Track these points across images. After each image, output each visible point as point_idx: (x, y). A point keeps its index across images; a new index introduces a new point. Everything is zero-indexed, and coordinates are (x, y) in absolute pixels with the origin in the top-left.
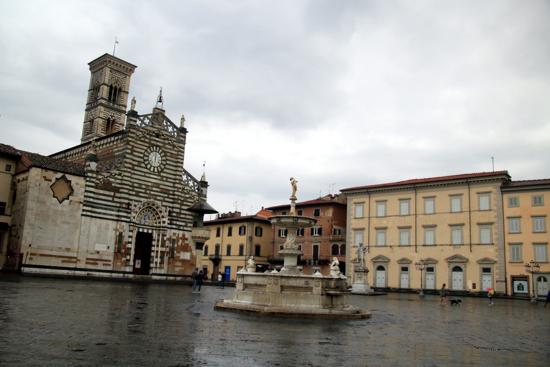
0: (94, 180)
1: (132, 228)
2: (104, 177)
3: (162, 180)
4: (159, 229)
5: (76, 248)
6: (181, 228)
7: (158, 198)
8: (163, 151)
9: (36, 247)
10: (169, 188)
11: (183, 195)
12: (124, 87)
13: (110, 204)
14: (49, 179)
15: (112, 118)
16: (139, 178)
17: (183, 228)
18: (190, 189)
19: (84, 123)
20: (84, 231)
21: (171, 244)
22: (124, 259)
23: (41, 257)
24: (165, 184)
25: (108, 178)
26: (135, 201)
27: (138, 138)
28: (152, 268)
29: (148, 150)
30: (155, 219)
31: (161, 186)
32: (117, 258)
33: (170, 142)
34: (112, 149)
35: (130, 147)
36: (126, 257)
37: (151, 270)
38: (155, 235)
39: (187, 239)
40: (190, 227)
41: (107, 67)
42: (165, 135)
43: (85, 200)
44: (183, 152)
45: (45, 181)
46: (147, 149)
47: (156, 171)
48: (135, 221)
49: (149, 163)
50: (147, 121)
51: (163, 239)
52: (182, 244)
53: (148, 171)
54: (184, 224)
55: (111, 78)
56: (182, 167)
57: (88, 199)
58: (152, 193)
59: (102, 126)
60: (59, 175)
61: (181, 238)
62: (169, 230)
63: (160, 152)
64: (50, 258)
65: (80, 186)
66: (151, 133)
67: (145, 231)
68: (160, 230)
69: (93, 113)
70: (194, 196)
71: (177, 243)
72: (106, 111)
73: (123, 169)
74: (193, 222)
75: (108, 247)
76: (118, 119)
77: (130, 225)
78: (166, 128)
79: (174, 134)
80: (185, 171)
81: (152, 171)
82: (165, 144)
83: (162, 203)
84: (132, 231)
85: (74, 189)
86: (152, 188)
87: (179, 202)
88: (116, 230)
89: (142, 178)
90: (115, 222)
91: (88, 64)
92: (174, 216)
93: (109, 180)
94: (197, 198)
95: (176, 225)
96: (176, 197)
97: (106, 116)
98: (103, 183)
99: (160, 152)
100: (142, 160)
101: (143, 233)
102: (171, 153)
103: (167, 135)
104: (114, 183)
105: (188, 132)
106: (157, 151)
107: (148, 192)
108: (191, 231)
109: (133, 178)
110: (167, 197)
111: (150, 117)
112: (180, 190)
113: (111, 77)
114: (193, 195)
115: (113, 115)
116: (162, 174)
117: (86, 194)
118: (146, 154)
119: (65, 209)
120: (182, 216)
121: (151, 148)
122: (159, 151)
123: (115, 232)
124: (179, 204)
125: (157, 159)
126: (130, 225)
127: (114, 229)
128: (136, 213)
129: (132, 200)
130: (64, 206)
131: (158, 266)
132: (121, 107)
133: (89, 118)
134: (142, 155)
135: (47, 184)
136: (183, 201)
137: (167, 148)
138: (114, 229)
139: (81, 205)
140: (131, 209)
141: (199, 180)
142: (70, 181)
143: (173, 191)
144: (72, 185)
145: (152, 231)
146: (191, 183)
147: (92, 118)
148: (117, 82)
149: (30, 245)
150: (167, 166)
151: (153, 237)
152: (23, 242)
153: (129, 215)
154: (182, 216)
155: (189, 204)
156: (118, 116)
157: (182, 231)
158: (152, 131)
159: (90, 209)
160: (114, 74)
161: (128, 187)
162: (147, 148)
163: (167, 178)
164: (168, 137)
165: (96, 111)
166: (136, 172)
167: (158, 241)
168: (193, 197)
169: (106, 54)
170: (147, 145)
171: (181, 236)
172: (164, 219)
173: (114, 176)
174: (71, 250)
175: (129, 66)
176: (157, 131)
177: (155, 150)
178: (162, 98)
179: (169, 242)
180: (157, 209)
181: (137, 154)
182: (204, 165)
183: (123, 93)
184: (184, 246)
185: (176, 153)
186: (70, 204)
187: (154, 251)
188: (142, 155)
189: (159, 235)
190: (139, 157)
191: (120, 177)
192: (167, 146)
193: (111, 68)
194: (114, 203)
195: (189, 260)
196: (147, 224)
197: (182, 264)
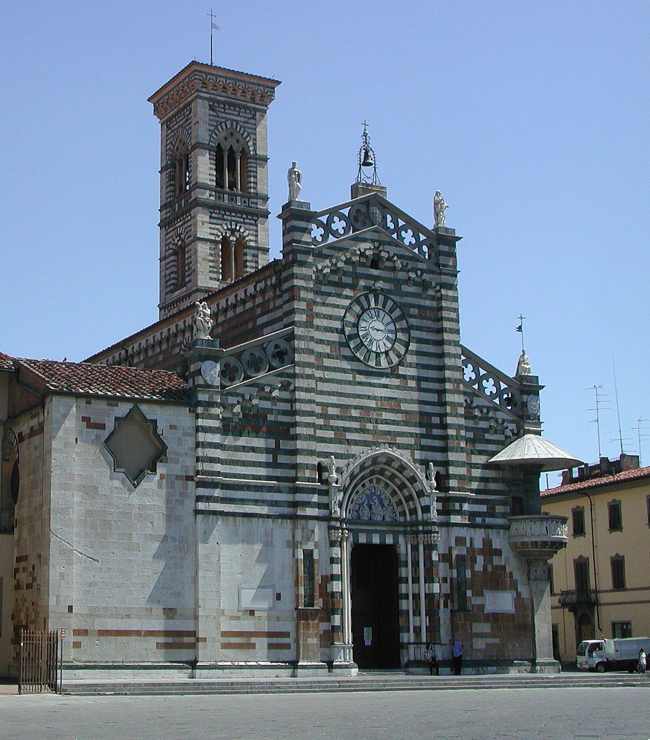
2: (243, 398)
4: (414, 529)
5: (192, 606)
6: (479, 520)
7: (400, 440)
8: (396, 305)
9: (86, 611)
10: (429, 409)
12: (255, 145)
14: (98, 421)
15: (233, 234)
17: (483, 521)
18: (491, 405)
19: (161, 260)
21: (455, 571)
22: (324, 626)
23: (102, 638)
26: (338, 456)
27: (321, 278)
28: (405, 646)
30: (399, 503)
31: (404, 406)
32: (307, 626)
33: (412, 275)
34: (254, 319)
35: (303, 305)
37: (403, 652)
38: (402, 550)
39: (498, 553)
40: (504, 515)
41: (200, 97)
43: (200, 468)
44: (455, 299)
50: (339, 225)
51: (428, 557)
52: (485, 567)
53: (362, 367)
54: (483, 508)
55: (216, 127)
56: (457, 344)
57: (207, 466)
58: (381, 427)
59: (210, 261)
60: (123, 409)
61: (482, 552)
64: (124, 639)
65: (181, 432)
66: (355, 259)
67: (376, 540)
68: (417, 533)
69: (179, 231)
72: (214, 218)
73: (291, 371)
74: (510, 500)
75: (278, 597)
76: (249, 235)
78: (395, 236)
79: (420, 250)
80: (465, 352)
82: (398, 283)
83: (413, 455)
85: (165, 442)
87: (463, 444)
88: (293, 545)
89: (348, 389)
90: (288, 523)
91: (149, 100)
92: (453, 489)
94: (512, 426)
96: (451, 432)
97: (215, 232)
98: (241, 416)
101: (369, 546)
102: (419, 307)
103: (400, 257)
105: (459, 239)
107: (370, 426)
108: (507, 528)
111: (346, 212)
113: (215, 123)
114: (500, 421)
115: (233, 227)
117: (200, 452)
119: (148, 502)
122: (384, 306)
123: (291, 550)
124: (462, 450)
126: (330, 528)
127: (288, 542)
129: (327, 455)
131: (424, 640)
132: (255, 201)
133: (171, 246)
134: (337, 325)
135: (94, 438)
137: (407, 294)
138: (288, 542)
139: (191, 484)
140: (326, 482)
141: (512, 374)
142: (154, 422)
144: (159, 432)
145: (396, 539)
146: (489, 387)
147: (180, 243)
148: (232, 134)
149: (70, 609)
151: (396, 555)
152: (52, 602)
153: (325, 500)
155: (491, 447)
156: (247, 226)
157: (483, 530)
158: (358, 252)
160: (220, 114)
162: (350, 301)
165: (189, 224)
166: (328, 375)
167: (416, 564)
168: (499, 428)
169: (194, 63)
171: (478, 544)
172: (425, 501)
173: (271, 392)
174: (179, 611)
175: (259, 85)
176: (370, 249)
178: (370, 153)
179: (448, 564)
180: (401, 473)
181: (325, 323)
182: (520, 329)
183: (252, 161)
185: (434, 304)
186: (160, 487)
187: (406, 596)
189: (415, 548)
191: (286, 395)
192: (405, 288)
193: (210, 99)
194: (280, 470)
196: (379, 518)
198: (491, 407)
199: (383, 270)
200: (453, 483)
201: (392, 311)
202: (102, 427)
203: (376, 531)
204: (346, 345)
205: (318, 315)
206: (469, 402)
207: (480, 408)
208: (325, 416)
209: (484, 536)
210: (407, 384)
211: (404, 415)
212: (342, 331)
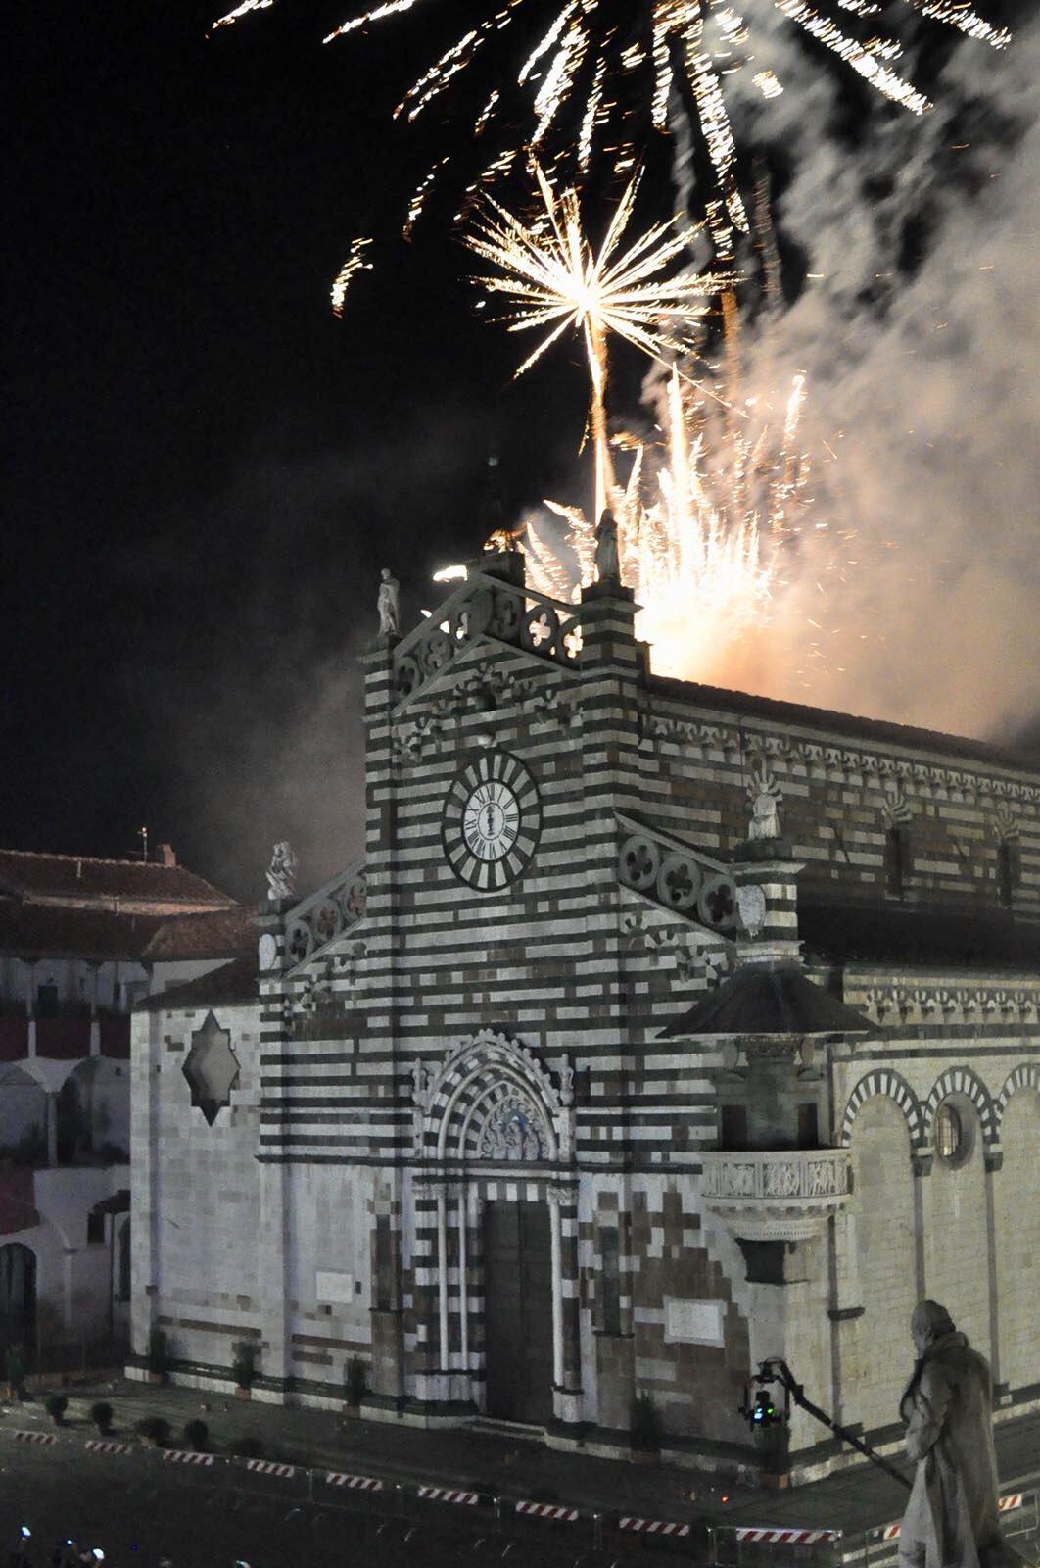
3: (531, 917)
7: (525, 1016)
8: (523, 764)
10: (571, 949)
11: (643, 964)
13: (345, 1091)
17: (666, 1158)
20: (268, 1226)
29: (459, 790)
31: (532, 952)
33: (540, 701)
35: (376, 814)
36: (415, 1331)
39: (693, 1222)
42: (512, 680)
46: (452, 787)
47: (500, 879)
49: (469, 852)
52: (667, 1250)
54: (665, 1133)
58: (497, 996)
60: (201, 1015)
61: (661, 1220)
62: (585, 1177)
63: (506, 780)
64: (203, 1333)
67: (512, 1193)
71: (643, 1252)
75: (358, 1288)
77: (416, 1179)
82: (522, 723)
83: (543, 1039)
86: (496, 974)
89: (449, 938)
93: (328, 989)
94: (718, 958)
95: (608, 1145)
98: (314, 1009)
99: (506, 780)
100: (437, 851)
102: (558, 757)
103: (519, 674)
106: (496, 776)
107: (478, 998)
112: (612, 945)
116: (529, 886)
118: (452, 812)
119: (225, 1144)
120: (651, 1088)
121: (470, 771)
125: (497, 814)
128: (437, 1113)
130: (219, 1133)
134: (432, 829)
135: (173, 1063)
136: (650, 999)
142: (227, 1031)
143: (585, 958)
145: (542, 1192)
150: (549, 835)
154: (651, 1088)
157: (663, 1176)
158: (456, 693)
159: (274, 1130)
161: (386, 1002)
163: (552, 896)
164: (525, 682)
168: (698, 963)
170: (451, 767)
171: (655, 1205)
177: (485, 778)
186: (233, 1124)
188: (432, 829)
191: (363, 965)
196: (514, 1156)
197: (681, 1374)
198: (675, 925)
199: (501, 707)
200: (597, 1089)
201: (513, 779)
202: (179, 1047)
203: (512, 1179)
206: (633, 922)
207: (654, 931)
208: (419, 991)
209: (665, 1190)
212: (439, 839)
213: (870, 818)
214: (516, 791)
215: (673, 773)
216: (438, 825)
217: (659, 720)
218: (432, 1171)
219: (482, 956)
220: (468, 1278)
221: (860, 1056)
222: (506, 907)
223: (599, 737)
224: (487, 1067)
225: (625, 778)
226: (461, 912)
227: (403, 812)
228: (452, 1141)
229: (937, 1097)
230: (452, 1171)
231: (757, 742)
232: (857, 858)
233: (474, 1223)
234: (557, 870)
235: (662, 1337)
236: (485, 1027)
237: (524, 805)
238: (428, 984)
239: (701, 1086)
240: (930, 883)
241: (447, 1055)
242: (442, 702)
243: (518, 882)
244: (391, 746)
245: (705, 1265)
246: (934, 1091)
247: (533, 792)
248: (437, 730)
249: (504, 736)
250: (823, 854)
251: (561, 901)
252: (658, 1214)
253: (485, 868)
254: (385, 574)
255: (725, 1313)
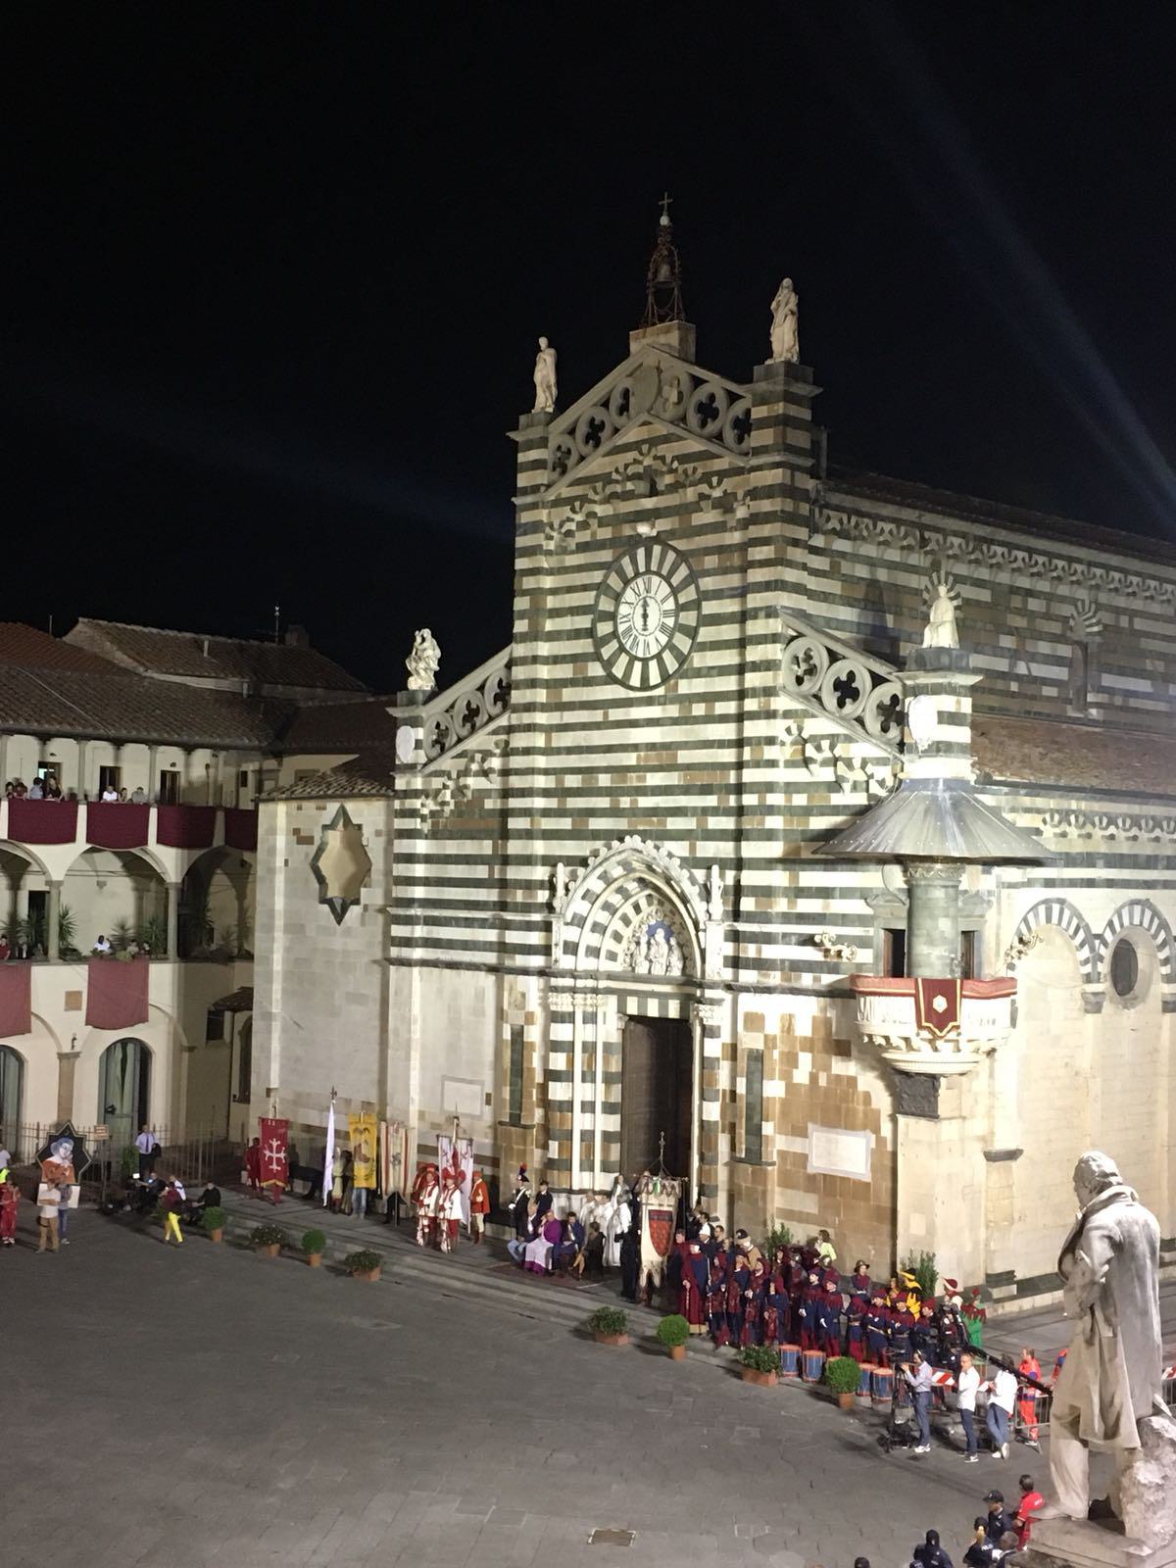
0: (417, 803)
1: (562, 1003)
7: (674, 824)
8: (683, 556)
11: (800, 775)
16: (583, 744)
20: (396, 1030)
24: (703, 737)
25: (462, 781)
29: (614, 581)
31: (684, 757)
33: (704, 488)
42: (675, 464)
45: (300, 846)
46: (606, 577)
47: (655, 677)
48: (585, 963)
49: (622, 649)
52: (814, 1078)
53: (618, 692)
58: (645, 802)
61: (808, 1045)
63: (664, 572)
66: (609, 489)
67: (653, 1010)
70: (863, 767)
81: (638, 684)
82: (684, 510)
83: (693, 849)
84: (568, 1018)
93: (466, 787)
94: (884, 773)
95: (760, 964)
96: (749, 800)
98: (452, 807)
102: (720, 550)
103: (683, 459)
104: (490, 797)
107: (625, 802)
109: (558, 751)
110: (715, 811)
112: (770, 752)
114: (857, 763)
116: (685, 687)
118: (605, 605)
119: (353, 944)
121: (626, 561)
124: (769, 835)
125: (653, 611)
128: (579, 921)
130: (348, 932)
134: (583, 622)
135: (303, 856)
136: (807, 811)
137: (703, 530)
142: (360, 827)
144: (364, 843)
150: (706, 634)
163: (710, 698)
164: (690, 467)
166: (570, 717)
170: (606, 556)
171: (804, 1029)
173: (483, 760)
176: (636, 462)
177: (642, 569)
184: (827, 1090)
186: (363, 923)
188: (583, 622)
190: (576, 634)
192: (699, 519)
195: (868, 1184)
196: (658, 970)
197: (823, 1208)
198: (838, 735)
199: (662, 493)
200: (747, 904)
202: (309, 840)
204: (595, 656)
205: (556, 613)
206: (795, 731)
207: (816, 740)
210: (690, 711)
211: (682, 773)
212: (590, 633)
213: (1055, 628)
214: (675, 585)
215: (843, 572)
216: (592, 616)
217: (832, 513)
218: (568, 982)
219: (631, 759)
220: (607, 1092)
221: (1030, 883)
222: (660, 708)
223: (766, 530)
224: (632, 876)
225: (791, 575)
226: (610, 711)
227: (551, 602)
228: (594, 952)
229: (1113, 931)
230: (590, 983)
231: (937, 541)
232: (1039, 670)
233: (615, 1037)
234: (715, 672)
235: (805, 1168)
236: (631, 833)
237: (682, 600)
238: (575, 785)
239: (856, 907)
240: (1118, 701)
241: (591, 861)
242: (599, 485)
243: (672, 682)
244: (544, 532)
245: (853, 1094)
246: (1110, 924)
247: (692, 588)
248: (592, 515)
249: (663, 525)
250: (1002, 665)
251: (717, 704)
252: (805, 1038)
253: (638, 665)
254: (543, 342)
255: (873, 1145)
